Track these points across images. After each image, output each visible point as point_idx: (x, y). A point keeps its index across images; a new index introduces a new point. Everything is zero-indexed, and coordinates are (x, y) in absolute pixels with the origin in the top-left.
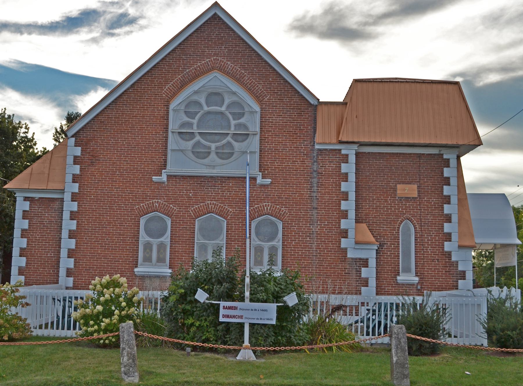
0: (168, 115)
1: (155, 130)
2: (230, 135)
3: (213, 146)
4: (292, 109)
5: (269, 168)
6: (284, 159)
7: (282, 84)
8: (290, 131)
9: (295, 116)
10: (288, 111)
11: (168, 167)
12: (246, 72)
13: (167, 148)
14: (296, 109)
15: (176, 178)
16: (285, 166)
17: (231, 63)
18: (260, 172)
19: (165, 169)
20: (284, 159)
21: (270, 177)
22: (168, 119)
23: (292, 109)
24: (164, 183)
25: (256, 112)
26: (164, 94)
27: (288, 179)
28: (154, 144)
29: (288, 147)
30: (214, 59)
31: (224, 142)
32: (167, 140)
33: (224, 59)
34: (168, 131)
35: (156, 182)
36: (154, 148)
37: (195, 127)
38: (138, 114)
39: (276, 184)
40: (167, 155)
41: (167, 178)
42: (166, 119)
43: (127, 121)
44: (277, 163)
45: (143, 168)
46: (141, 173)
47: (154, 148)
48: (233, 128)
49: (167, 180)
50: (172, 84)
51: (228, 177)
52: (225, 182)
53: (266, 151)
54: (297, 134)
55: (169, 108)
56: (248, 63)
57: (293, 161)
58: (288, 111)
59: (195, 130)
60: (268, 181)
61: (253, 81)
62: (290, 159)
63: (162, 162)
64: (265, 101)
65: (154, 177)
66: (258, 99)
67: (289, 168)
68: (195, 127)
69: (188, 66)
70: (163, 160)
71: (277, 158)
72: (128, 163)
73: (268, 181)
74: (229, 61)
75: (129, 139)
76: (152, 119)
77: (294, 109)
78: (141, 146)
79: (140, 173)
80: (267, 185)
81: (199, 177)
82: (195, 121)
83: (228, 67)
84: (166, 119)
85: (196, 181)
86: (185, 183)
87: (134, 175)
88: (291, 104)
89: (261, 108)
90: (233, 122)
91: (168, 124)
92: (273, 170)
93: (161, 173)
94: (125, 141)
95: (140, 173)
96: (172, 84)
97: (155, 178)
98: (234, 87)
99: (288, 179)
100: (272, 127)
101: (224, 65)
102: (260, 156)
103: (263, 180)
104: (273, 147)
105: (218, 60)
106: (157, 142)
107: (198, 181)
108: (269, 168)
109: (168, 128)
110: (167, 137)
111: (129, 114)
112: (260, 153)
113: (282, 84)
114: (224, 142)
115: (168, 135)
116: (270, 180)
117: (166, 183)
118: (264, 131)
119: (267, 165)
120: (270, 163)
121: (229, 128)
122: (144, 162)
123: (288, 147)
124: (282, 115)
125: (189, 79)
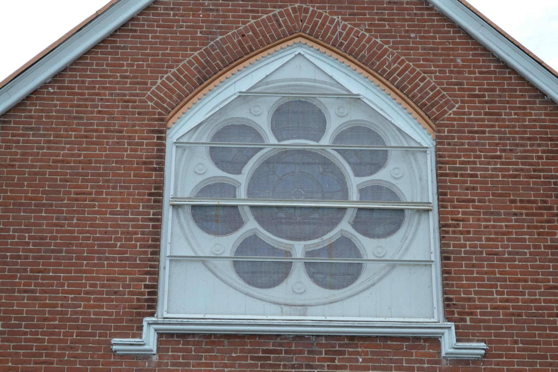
0: (163, 157)
1: (122, 200)
2: (349, 216)
3: (299, 249)
4: (529, 139)
5: (476, 307)
6: (519, 280)
7: (495, 73)
8: (529, 202)
9: (540, 158)
10: (517, 145)
11: (164, 310)
12: (387, 43)
13: (157, 253)
14: (542, 139)
15: (187, 343)
16: (524, 301)
17: (345, 20)
18: (449, 320)
19: (152, 315)
20: (519, 280)
21: (482, 335)
22: (162, 170)
23: (529, 139)
24: (146, 357)
25: (424, 150)
26: (151, 100)
27: (538, 343)
28: (117, 239)
29: (528, 247)
30: (294, 9)
31: (333, 235)
32: (159, 227)
33: (324, 8)
34: (161, 201)
35: (122, 356)
36: (119, 252)
37: (242, 192)
38: (73, 155)
39: (501, 356)
40: (157, 273)
41: (159, 342)
42: (155, 169)
43: (36, 173)
44: (498, 293)
45: (82, 313)
46: (78, 327)
47: (119, 252)
48: (354, 195)
49: (158, 349)
50: (174, 74)
51: (352, 338)
52: (343, 353)
53: (463, 259)
54: (551, 208)
55: (163, 139)
56: (393, 20)
57: (547, 288)
58: (517, 145)
59: (242, 198)
60: (476, 348)
61: (408, 66)
62: (537, 280)
63: (142, 294)
64: (449, 119)
65: (115, 340)
66: (426, 108)
67: (537, 308)
68: (242, 192)
69: (220, 28)
70: (146, 286)
71: (498, 280)
72: (36, 299)
73: (476, 348)
74: (337, 14)
75: (41, 225)
76: (112, 169)
77: (535, 139)
78: (81, 245)
79: (71, 327)
80: (475, 361)
81: (260, 336)
82: (242, 179)
83: (335, 29)
84: (155, 169)
85: (250, 351)
86: (215, 358)
87: (53, 334)
88: (526, 126)
89: (437, 137)
90: (355, 182)
91: (162, 182)
92: (490, 314)
93: (140, 328)
94: (28, 231)
95: (71, 327)
96: (174, 74)
97: (120, 344)
98: (354, 82)
99: (538, 343)
100: (474, 188)
101: (323, 24)
102: (444, 272)
103: (461, 344)
104: (482, 246)
105: (306, 10)
106: (129, 236)
107: (257, 351)
108: (476, 307)
109: (161, 195)
110: (160, 220)
111: (44, 154)
112: (443, 265)
113: (495, 73)
114: (333, 235)
115: (161, 214)
116: (482, 345)
117: (155, 358)
118: (451, 201)
119: (469, 300)
120: (476, 293)
121: (345, 196)
122: (87, 293)
123: (528, 247)
124: (500, 157)
125: (222, 61)
